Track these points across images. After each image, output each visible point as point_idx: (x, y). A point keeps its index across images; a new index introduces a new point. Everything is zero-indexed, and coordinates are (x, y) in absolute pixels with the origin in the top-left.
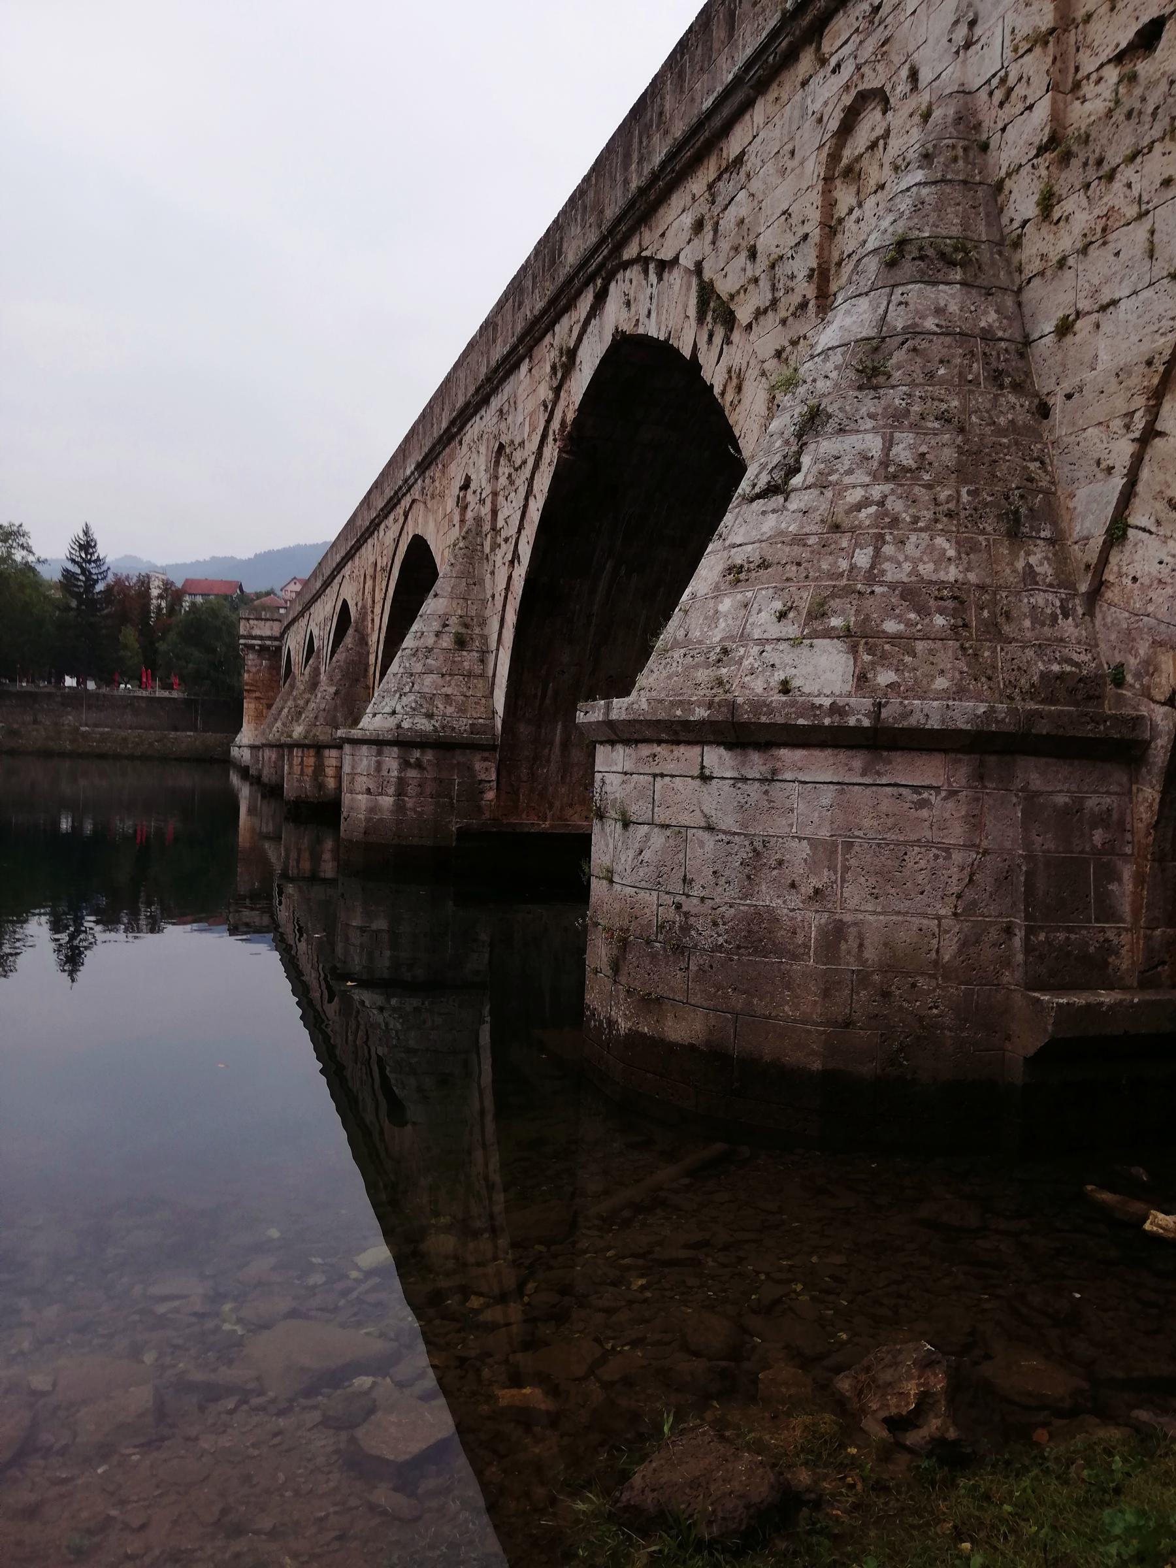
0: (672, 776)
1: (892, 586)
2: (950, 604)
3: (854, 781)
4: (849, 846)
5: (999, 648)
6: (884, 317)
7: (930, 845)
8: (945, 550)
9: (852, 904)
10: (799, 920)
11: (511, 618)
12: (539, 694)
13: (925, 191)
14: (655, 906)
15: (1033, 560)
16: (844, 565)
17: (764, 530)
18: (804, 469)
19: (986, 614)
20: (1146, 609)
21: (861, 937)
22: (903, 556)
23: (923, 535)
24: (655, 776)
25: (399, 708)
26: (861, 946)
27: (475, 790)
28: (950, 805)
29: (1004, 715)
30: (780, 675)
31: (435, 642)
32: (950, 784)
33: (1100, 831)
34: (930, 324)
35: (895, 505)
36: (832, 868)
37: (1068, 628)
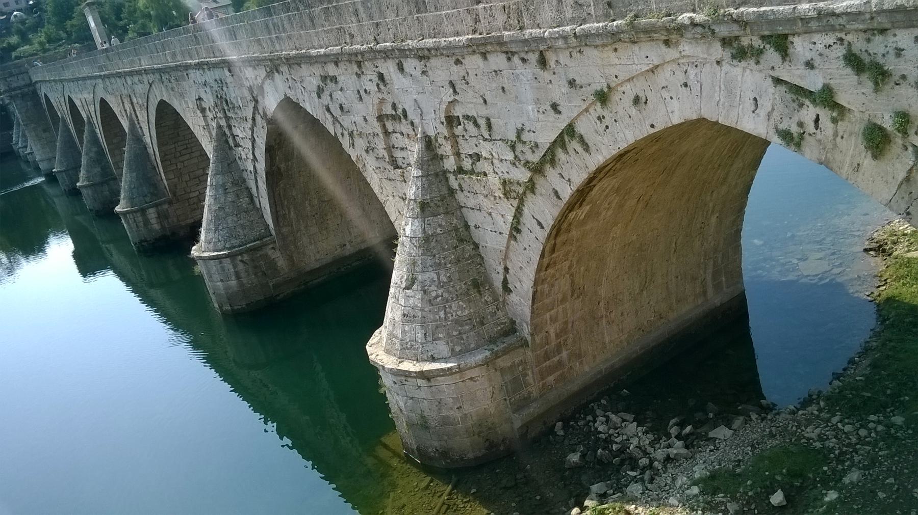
2: (469, 321)
6: (424, 229)
7: (481, 389)
12: (287, 213)
13: (424, 179)
15: (486, 298)
16: (438, 317)
19: (478, 320)
23: (456, 302)
25: (220, 238)
27: (272, 264)
28: (483, 379)
30: (430, 354)
31: (225, 199)
34: (438, 231)
35: (446, 295)
37: (500, 313)
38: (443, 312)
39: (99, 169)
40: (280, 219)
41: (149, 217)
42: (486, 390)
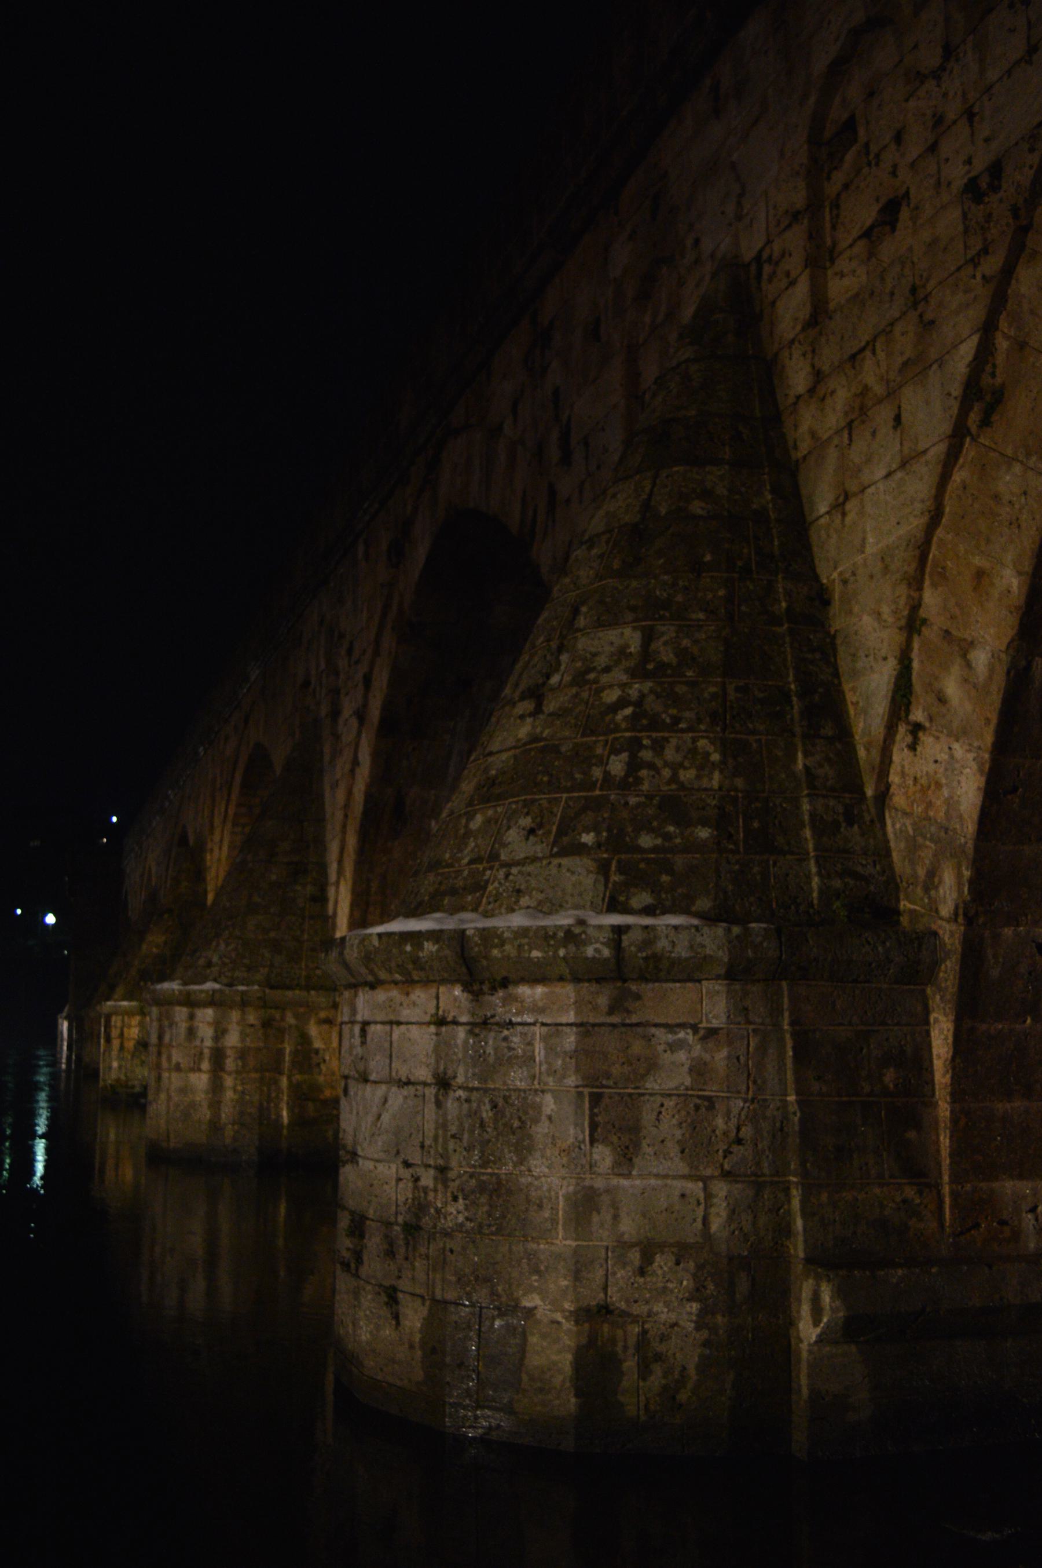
0: (407, 1023)
1: (650, 797)
5: (771, 862)
8: (707, 754)
10: (545, 1189)
11: (352, 841)
14: (394, 1183)
17: (520, 736)
18: (563, 667)
19: (756, 825)
20: (927, 813)
21: (615, 1206)
22: (662, 762)
24: (391, 1023)
25: (215, 959)
29: (759, 939)
32: (708, 1021)
33: (892, 1070)
34: (697, 507)
38: (625, 756)
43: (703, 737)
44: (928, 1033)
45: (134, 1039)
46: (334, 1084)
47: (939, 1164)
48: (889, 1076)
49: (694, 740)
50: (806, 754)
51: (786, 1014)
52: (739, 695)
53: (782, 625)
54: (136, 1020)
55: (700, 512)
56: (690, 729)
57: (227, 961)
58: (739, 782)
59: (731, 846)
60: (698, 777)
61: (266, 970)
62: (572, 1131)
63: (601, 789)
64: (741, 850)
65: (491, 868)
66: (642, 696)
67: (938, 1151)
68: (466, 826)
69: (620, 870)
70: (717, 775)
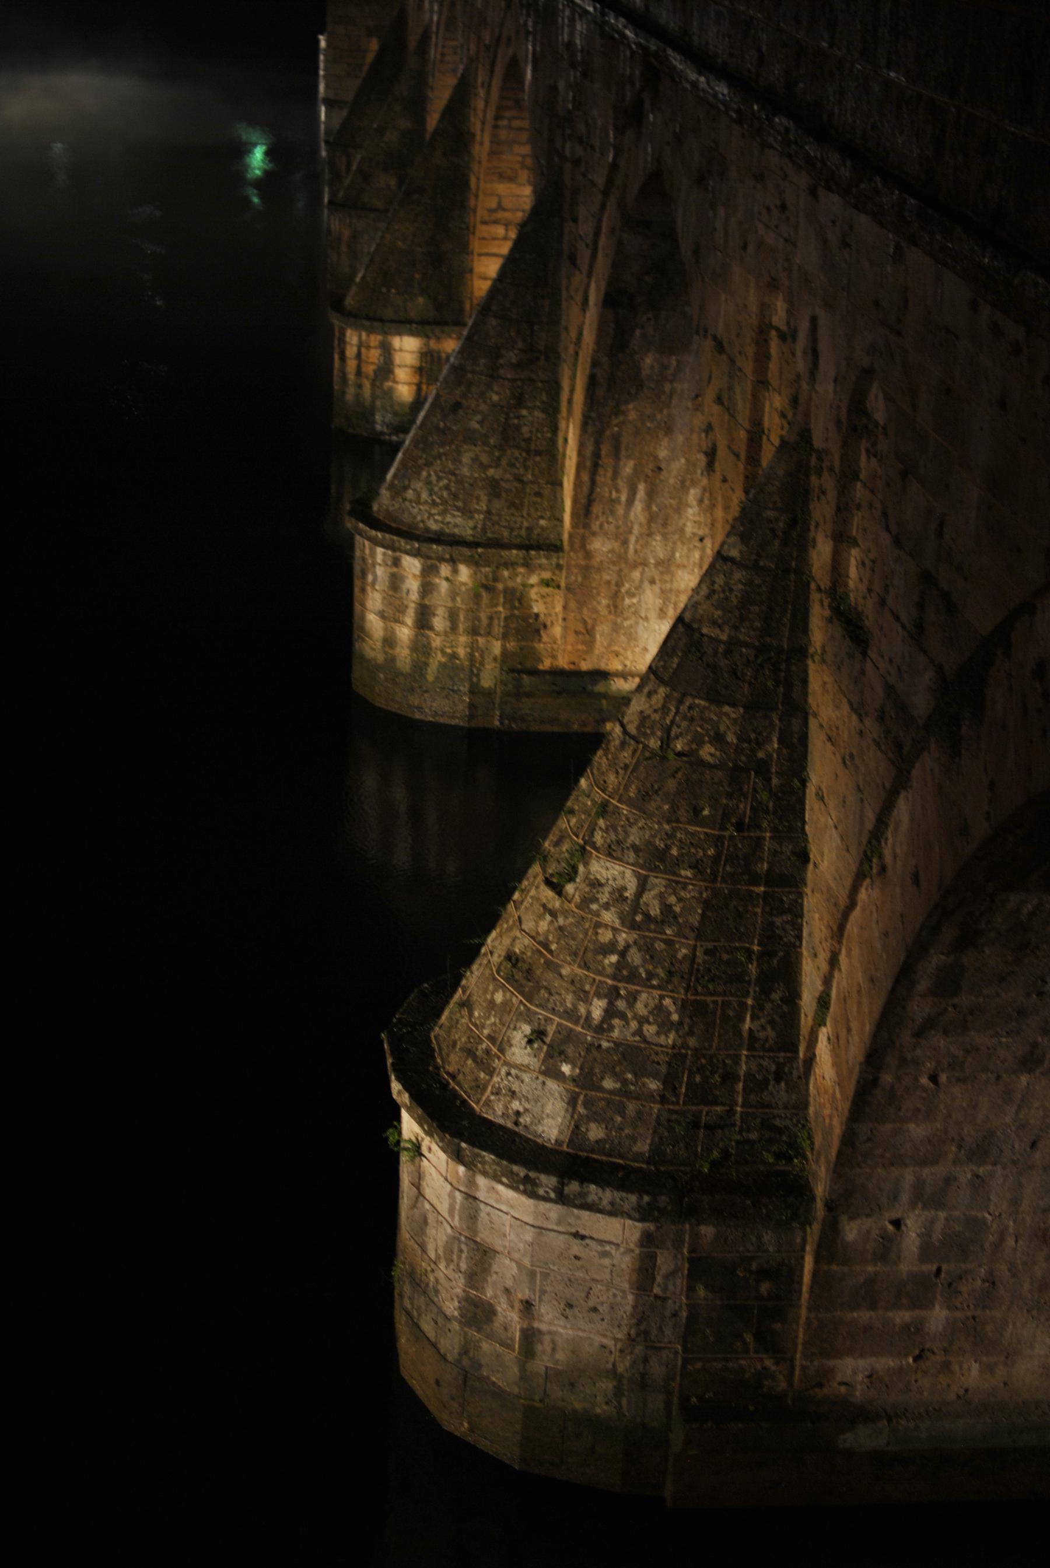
1: (617, 1044)
3: (550, 1227)
4: (546, 1276)
5: (704, 1113)
9: (546, 1318)
12: (624, 498)
13: (738, 575)
16: (582, 1010)
19: (698, 1079)
21: (553, 1342)
23: (656, 993)
26: (554, 1349)
32: (627, 1243)
34: (707, 752)
35: (635, 957)
36: (532, 1290)
38: (605, 1001)
39: (393, 183)
40: (596, 509)
41: (398, 358)
42: (624, 1297)
43: (667, 996)
44: (803, 1258)
45: (374, 363)
46: (555, 653)
47: (796, 1345)
48: (765, 1288)
49: (662, 997)
50: (752, 1019)
51: (686, 1245)
52: (706, 958)
53: (759, 885)
54: (375, 339)
55: (710, 759)
56: (659, 987)
57: (438, 501)
58: (692, 1042)
59: (674, 1099)
60: (658, 1034)
61: (482, 516)
62: (527, 1291)
63: (583, 1028)
64: (681, 1102)
65: (499, 1058)
66: (628, 947)
67: (797, 1337)
68: (493, 994)
69: (587, 1104)
70: (672, 1035)
